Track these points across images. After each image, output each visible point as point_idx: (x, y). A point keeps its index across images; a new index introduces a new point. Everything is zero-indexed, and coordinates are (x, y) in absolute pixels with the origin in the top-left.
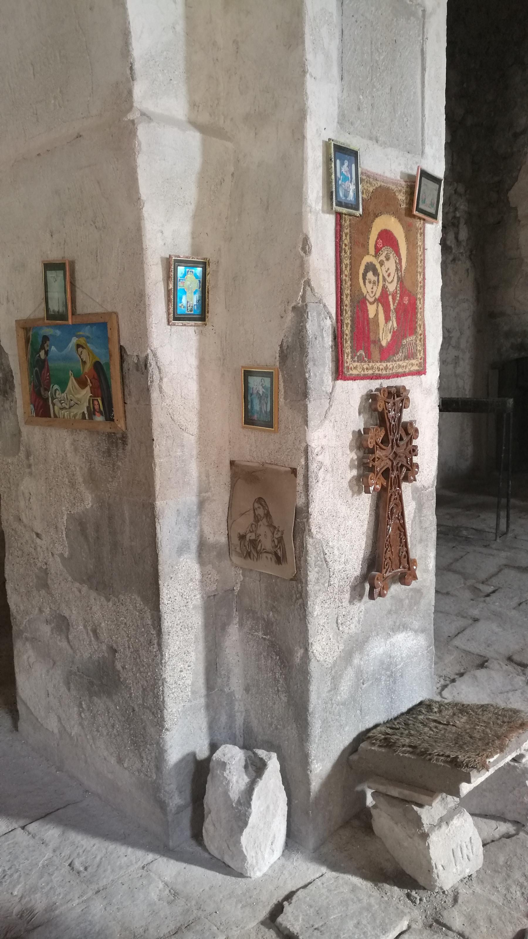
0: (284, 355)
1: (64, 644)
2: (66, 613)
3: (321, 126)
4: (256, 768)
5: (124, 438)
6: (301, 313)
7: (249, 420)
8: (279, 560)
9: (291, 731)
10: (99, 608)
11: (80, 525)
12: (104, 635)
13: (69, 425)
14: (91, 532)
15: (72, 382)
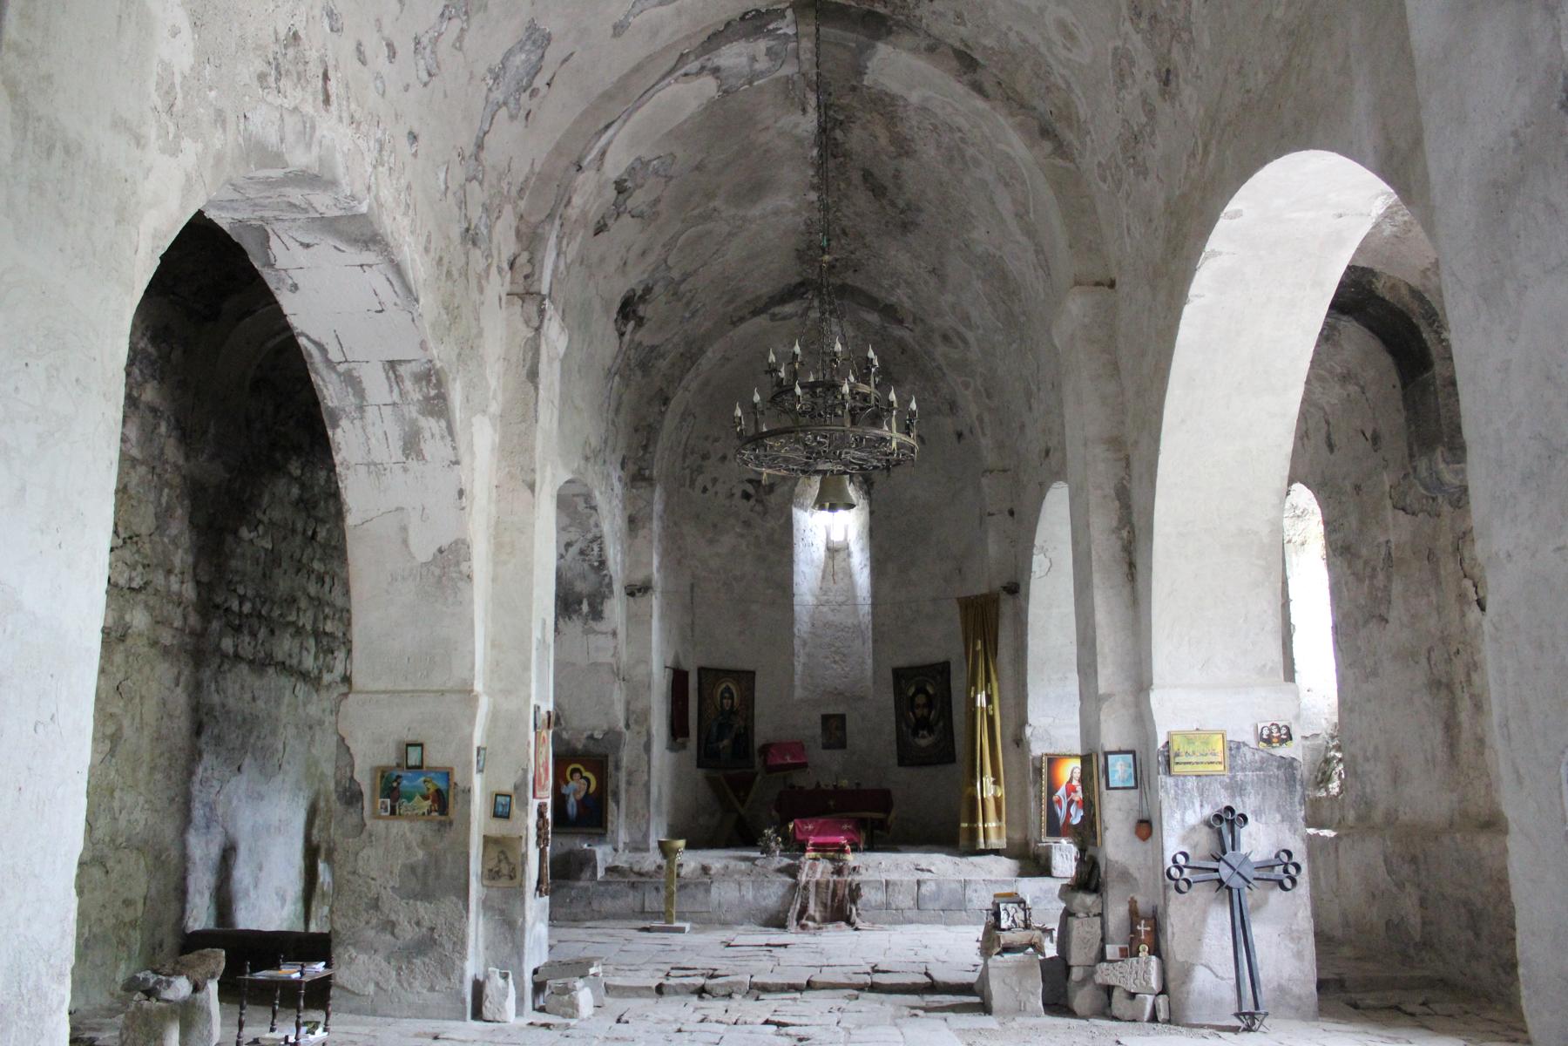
0: (516, 788)
1: (388, 937)
2: (393, 917)
3: (533, 701)
4: (505, 977)
5: (451, 823)
6: (525, 771)
7: (496, 815)
8: (511, 878)
9: (515, 960)
10: (423, 909)
11: (413, 869)
12: (427, 923)
13: (411, 819)
14: (420, 871)
15: (418, 798)
